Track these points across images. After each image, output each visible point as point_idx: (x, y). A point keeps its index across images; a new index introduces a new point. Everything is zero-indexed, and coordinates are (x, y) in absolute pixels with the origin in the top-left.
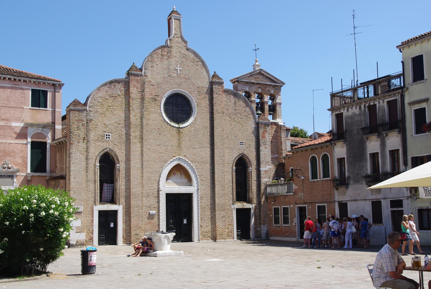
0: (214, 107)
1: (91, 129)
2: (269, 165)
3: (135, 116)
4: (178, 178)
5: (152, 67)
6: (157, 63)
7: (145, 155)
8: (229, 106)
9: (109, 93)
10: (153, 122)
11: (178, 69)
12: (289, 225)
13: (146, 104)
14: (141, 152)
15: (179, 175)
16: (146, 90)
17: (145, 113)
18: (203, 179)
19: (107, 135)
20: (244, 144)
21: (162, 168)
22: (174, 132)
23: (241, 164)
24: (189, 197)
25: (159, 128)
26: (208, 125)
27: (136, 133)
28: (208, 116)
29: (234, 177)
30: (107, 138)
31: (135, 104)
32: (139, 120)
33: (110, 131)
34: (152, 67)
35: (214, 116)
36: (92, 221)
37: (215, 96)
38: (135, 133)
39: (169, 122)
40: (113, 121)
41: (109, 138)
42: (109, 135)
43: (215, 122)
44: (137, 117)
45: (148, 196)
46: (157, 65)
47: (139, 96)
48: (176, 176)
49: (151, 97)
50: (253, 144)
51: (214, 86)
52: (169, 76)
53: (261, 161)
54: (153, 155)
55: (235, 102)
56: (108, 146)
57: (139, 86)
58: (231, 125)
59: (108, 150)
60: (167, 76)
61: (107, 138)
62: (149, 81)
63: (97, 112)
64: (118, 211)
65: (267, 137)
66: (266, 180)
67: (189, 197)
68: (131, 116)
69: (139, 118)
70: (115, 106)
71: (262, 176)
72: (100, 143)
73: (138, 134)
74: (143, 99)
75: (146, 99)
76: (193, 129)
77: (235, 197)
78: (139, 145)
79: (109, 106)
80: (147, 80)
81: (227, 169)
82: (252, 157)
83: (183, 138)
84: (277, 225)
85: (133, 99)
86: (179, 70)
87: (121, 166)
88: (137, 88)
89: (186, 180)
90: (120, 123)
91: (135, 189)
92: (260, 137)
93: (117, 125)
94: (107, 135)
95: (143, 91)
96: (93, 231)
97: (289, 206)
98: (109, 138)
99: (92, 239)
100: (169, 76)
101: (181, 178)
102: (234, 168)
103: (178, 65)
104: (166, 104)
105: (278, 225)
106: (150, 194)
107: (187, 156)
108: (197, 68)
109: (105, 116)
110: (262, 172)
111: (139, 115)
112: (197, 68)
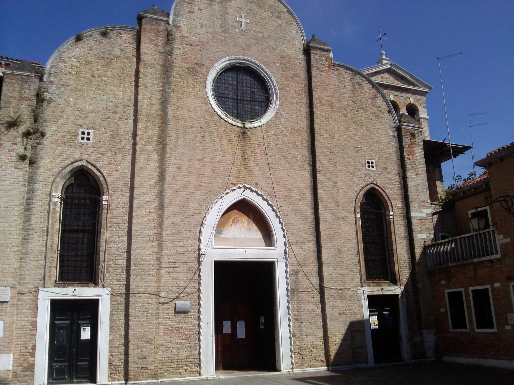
0: (314, 93)
1: (47, 118)
2: (427, 207)
3: (148, 98)
4: (243, 229)
5: (190, 12)
6: (201, 7)
7: (168, 179)
8: (343, 94)
9: (95, 52)
10: (190, 114)
11: (243, 20)
12: (495, 330)
13: (175, 78)
14: (158, 170)
15: (246, 224)
16: (176, 52)
17: (172, 94)
18: (295, 232)
19: (83, 133)
20: (374, 165)
21: (207, 207)
22: (235, 135)
23: (373, 204)
24: (266, 269)
25: (202, 125)
26: (304, 125)
27: (151, 132)
28: (304, 109)
29: (360, 229)
30: (83, 138)
31: (151, 78)
32: (158, 107)
33: (91, 125)
34: (190, 12)
35: (315, 110)
36: (34, 325)
37: (314, 73)
38: (148, 131)
39: (223, 116)
40: (100, 107)
41: (88, 139)
42: (89, 134)
43: (316, 121)
44: (154, 101)
45: (173, 267)
46: (200, 10)
47: (159, 60)
48: (239, 225)
49: (186, 65)
50: (394, 168)
51: (312, 56)
52: (224, 32)
53: (410, 200)
54: (188, 179)
55: (354, 87)
56: (84, 156)
57: (161, 41)
58: (347, 129)
59: (84, 163)
60: (220, 31)
61: (83, 138)
62: (183, 37)
63: (65, 85)
64: (100, 301)
65: (418, 155)
66: (424, 236)
67: (266, 269)
68: (140, 97)
69: (158, 102)
70: (106, 76)
71: (414, 227)
72: (65, 149)
73: (153, 132)
74: (167, 69)
75: (175, 68)
76: (272, 132)
77: (363, 270)
78: (155, 157)
79: (94, 76)
80: (178, 34)
81: (343, 214)
82: (392, 192)
83: (252, 149)
84: (459, 330)
85: (145, 65)
86: (243, 23)
87: (114, 202)
88: (156, 45)
89: (258, 235)
90: (117, 110)
91: (144, 253)
92: (405, 154)
93: (107, 114)
94: (83, 133)
95: (170, 53)
96: (34, 348)
97: (488, 287)
98: (88, 139)
99: (31, 368)
100: (224, 32)
101: (249, 229)
102: (359, 211)
103: (243, 15)
104: (217, 81)
105: (464, 330)
106: (178, 263)
107: (261, 184)
108: (280, 22)
109: (83, 95)
110: (414, 221)
111: (158, 96)
112: (280, 22)
